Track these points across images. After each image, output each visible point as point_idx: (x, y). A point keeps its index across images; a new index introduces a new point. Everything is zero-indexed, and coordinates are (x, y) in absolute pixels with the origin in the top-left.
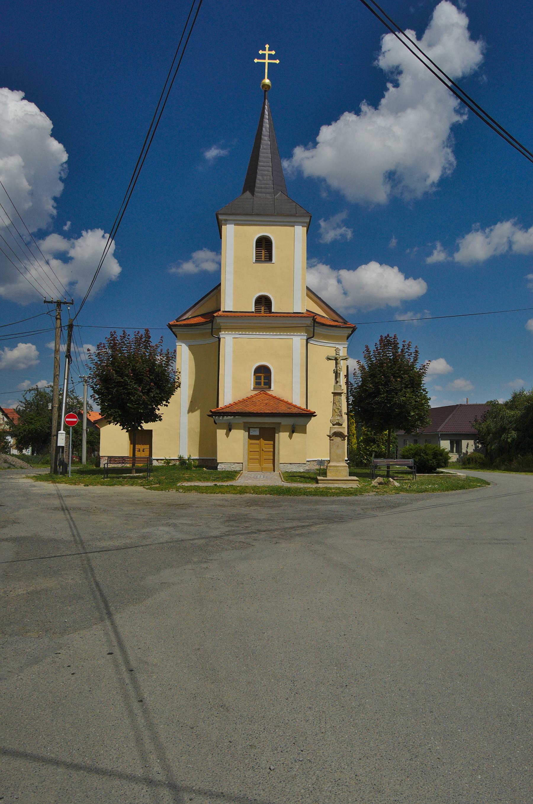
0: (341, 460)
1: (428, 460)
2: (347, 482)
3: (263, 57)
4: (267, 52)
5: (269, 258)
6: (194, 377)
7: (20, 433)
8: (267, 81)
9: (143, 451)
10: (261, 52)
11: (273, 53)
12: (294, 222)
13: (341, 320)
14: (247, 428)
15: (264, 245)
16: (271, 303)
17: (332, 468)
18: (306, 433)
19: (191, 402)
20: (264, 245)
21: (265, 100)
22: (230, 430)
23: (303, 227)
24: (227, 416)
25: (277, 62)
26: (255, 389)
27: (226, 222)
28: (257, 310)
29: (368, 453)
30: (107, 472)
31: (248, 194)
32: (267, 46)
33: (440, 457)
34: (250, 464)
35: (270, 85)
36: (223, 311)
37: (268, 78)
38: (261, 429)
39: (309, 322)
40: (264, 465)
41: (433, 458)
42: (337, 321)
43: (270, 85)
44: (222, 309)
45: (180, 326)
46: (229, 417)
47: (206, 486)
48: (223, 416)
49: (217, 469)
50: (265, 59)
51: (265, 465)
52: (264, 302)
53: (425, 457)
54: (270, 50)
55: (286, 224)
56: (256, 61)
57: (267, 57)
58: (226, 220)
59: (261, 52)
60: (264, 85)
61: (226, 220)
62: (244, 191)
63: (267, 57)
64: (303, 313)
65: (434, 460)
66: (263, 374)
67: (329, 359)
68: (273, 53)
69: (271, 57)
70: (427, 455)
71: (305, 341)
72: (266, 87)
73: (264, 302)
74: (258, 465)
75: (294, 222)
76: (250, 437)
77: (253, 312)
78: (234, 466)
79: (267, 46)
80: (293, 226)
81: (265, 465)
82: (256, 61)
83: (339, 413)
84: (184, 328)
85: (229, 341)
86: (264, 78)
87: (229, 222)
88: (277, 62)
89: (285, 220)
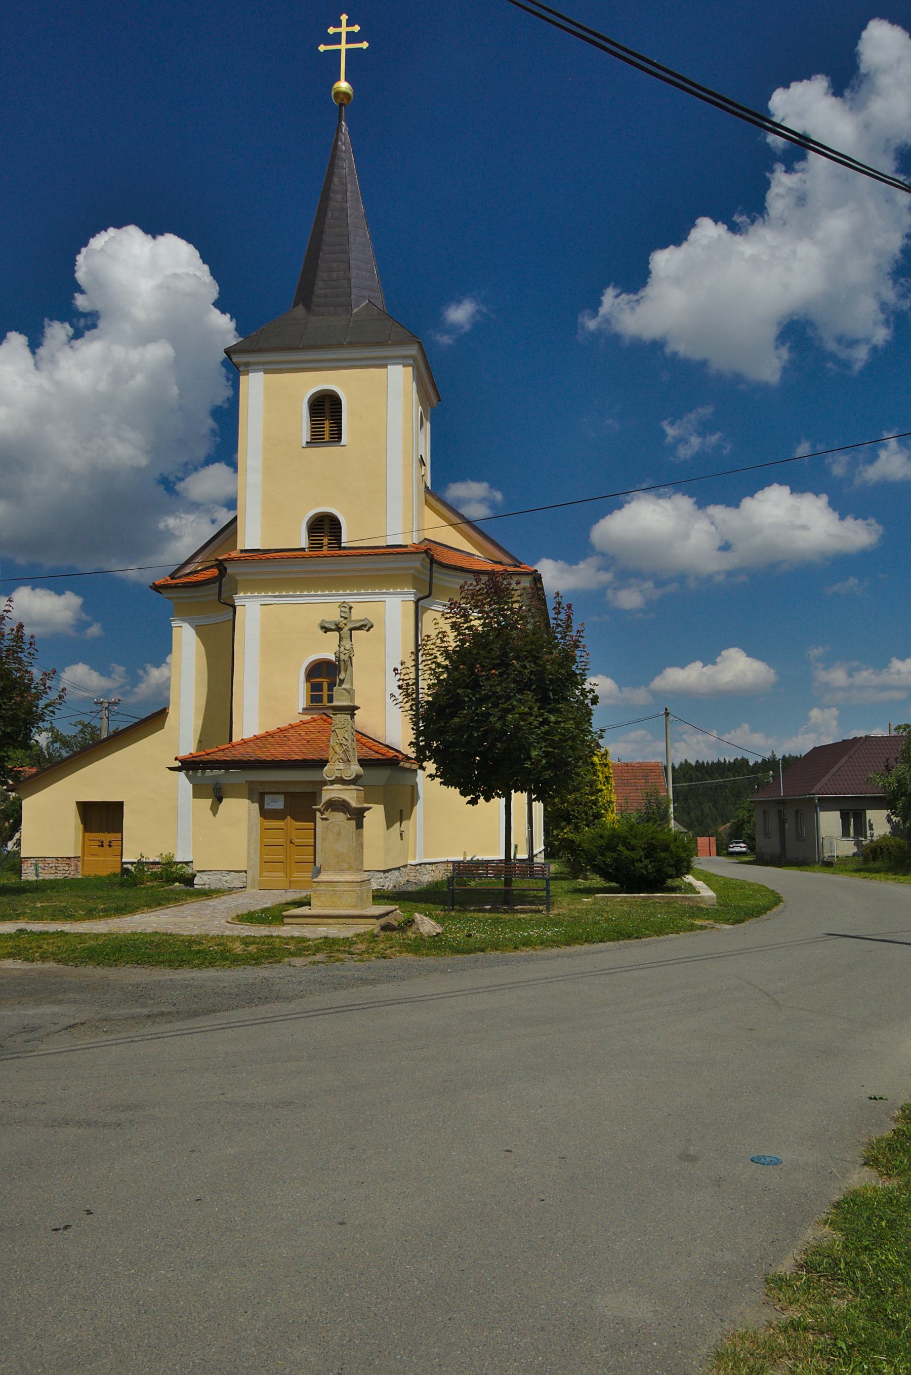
0: (345, 866)
1: (633, 861)
2: (350, 921)
3: (336, 39)
4: (344, 30)
5: (336, 436)
6: (205, 689)
7: (14, 811)
8: (343, 85)
9: (110, 846)
10: (331, 30)
11: (356, 28)
12: (386, 358)
13: (506, 560)
14: (258, 795)
15: (326, 410)
16: (339, 524)
17: (322, 887)
18: (120, 805)
19: (200, 741)
20: (326, 410)
21: (340, 121)
22: (220, 800)
23: (404, 366)
24: (212, 769)
25: (365, 45)
26: (306, 710)
27: (248, 367)
28: (315, 545)
29: (557, 843)
30: (38, 888)
31: (300, 310)
32: (344, 18)
33: (663, 855)
34: (265, 874)
35: (351, 93)
36: (242, 551)
37: (346, 80)
38: (288, 796)
39: (418, 563)
40: (296, 874)
41: (646, 857)
42: (501, 563)
43: (351, 93)
44: (239, 547)
45: (176, 586)
46: (216, 772)
47: (41, 933)
48: (204, 769)
49: (192, 885)
50: (340, 43)
51: (296, 876)
52: (325, 527)
53: (626, 853)
54: (349, 24)
55: (371, 363)
56: (322, 48)
57: (344, 36)
58: (247, 364)
59: (331, 30)
60: (338, 94)
61: (247, 364)
62: (296, 304)
63: (344, 36)
64: (406, 546)
65: (647, 862)
66: (324, 676)
67: (326, 630)
68: (356, 28)
69: (351, 37)
70: (633, 849)
71: (412, 606)
72: (342, 96)
73: (325, 527)
74: (282, 874)
75: (386, 358)
76: (265, 814)
77: (303, 549)
78: (228, 878)
79: (344, 18)
80: (385, 366)
81: (296, 876)
82: (322, 48)
83: (342, 756)
84: (185, 590)
85: (253, 612)
86: (339, 80)
87: (253, 367)
88: (365, 45)
89: (372, 354)
